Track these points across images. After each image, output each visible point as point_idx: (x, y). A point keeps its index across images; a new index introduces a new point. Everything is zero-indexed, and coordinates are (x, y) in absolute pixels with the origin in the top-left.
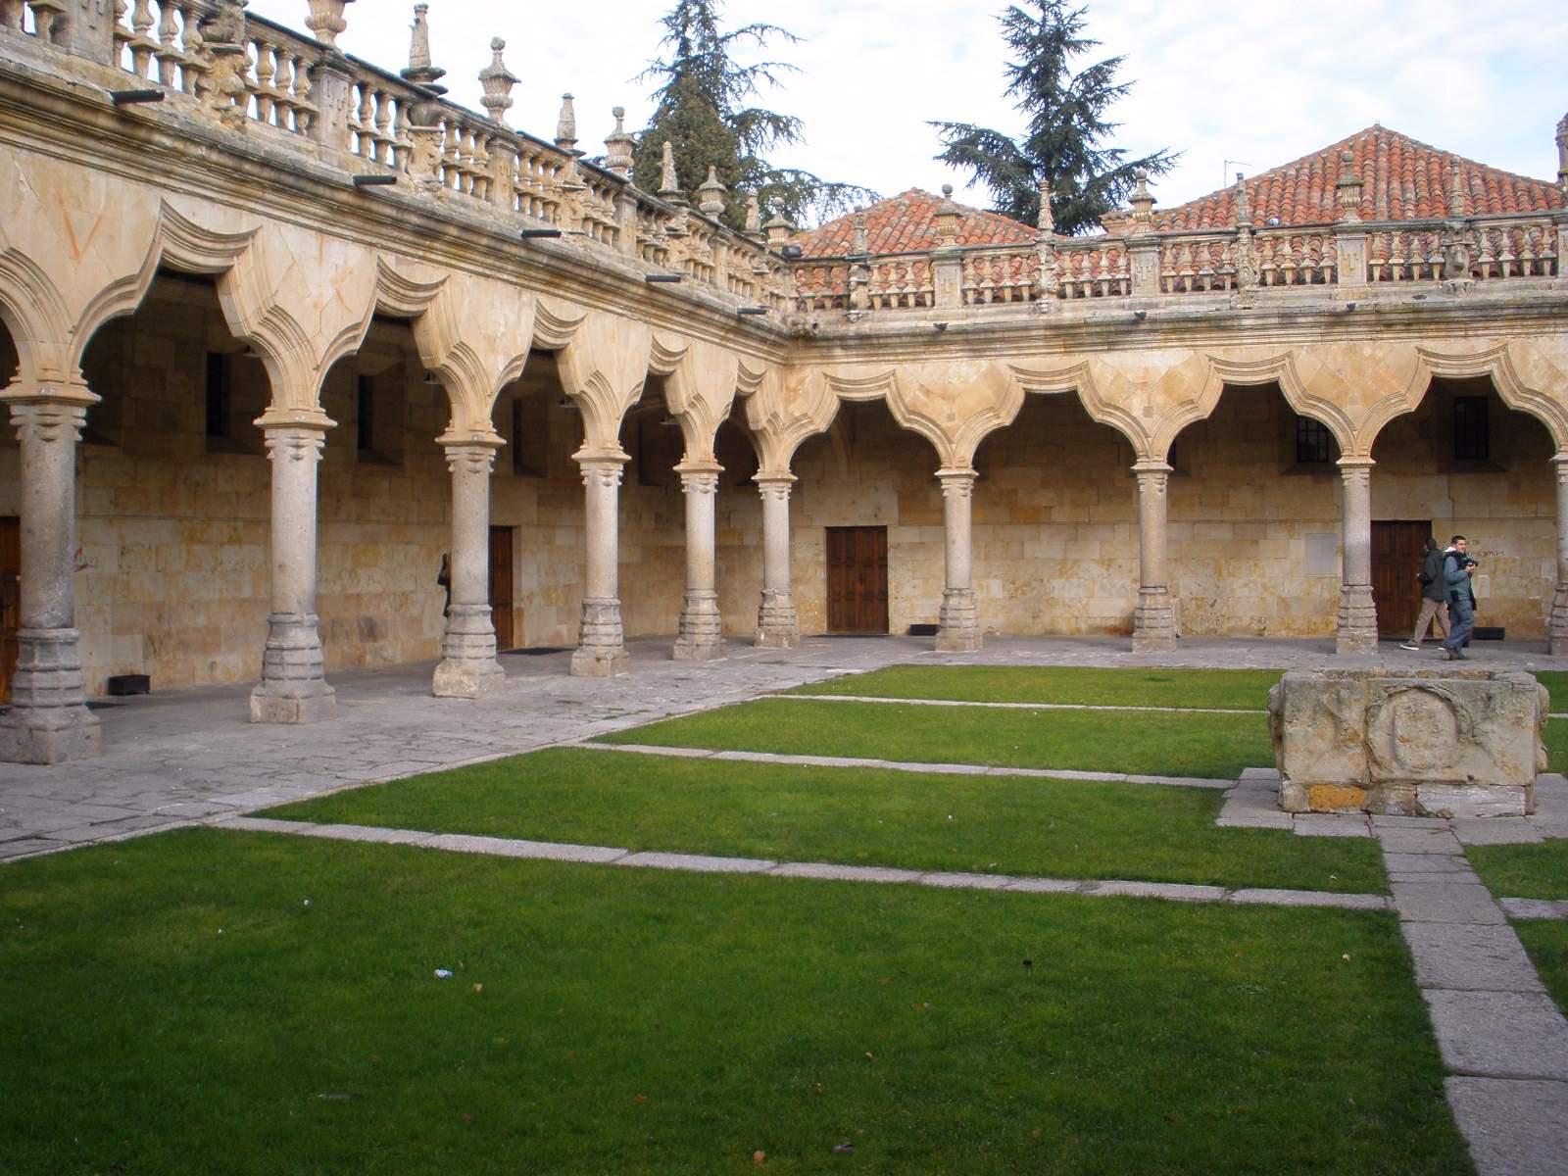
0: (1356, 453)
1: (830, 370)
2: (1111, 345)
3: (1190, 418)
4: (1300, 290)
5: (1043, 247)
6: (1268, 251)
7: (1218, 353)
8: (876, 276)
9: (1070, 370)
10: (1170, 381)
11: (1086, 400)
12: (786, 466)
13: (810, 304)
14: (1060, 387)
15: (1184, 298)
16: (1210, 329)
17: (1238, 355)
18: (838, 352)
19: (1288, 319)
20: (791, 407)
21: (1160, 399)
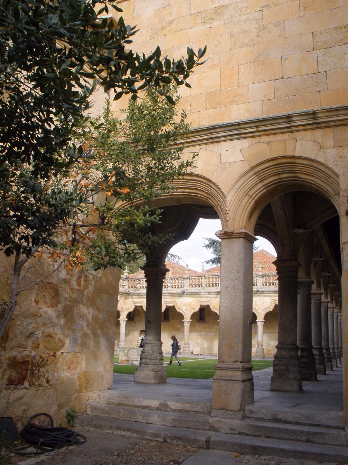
0: (187, 318)
1: (133, 300)
2: (180, 297)
3: (193, 311)
4: (213, 288)
5: (169, 278)
6: (208, 280)
7: (198, 299)
8: (141, 282)
9: (173, 302)
10: (190, 304)
11: (176, 307)
12: (126, 318)
13: (130, 287)
14: (172, 305)
15: (193, 289)
16: (196, 295)
17: (202, 300)
18: (134, 296)
19: (209, 293)
20: (126, 306)
21: (188, 307)
